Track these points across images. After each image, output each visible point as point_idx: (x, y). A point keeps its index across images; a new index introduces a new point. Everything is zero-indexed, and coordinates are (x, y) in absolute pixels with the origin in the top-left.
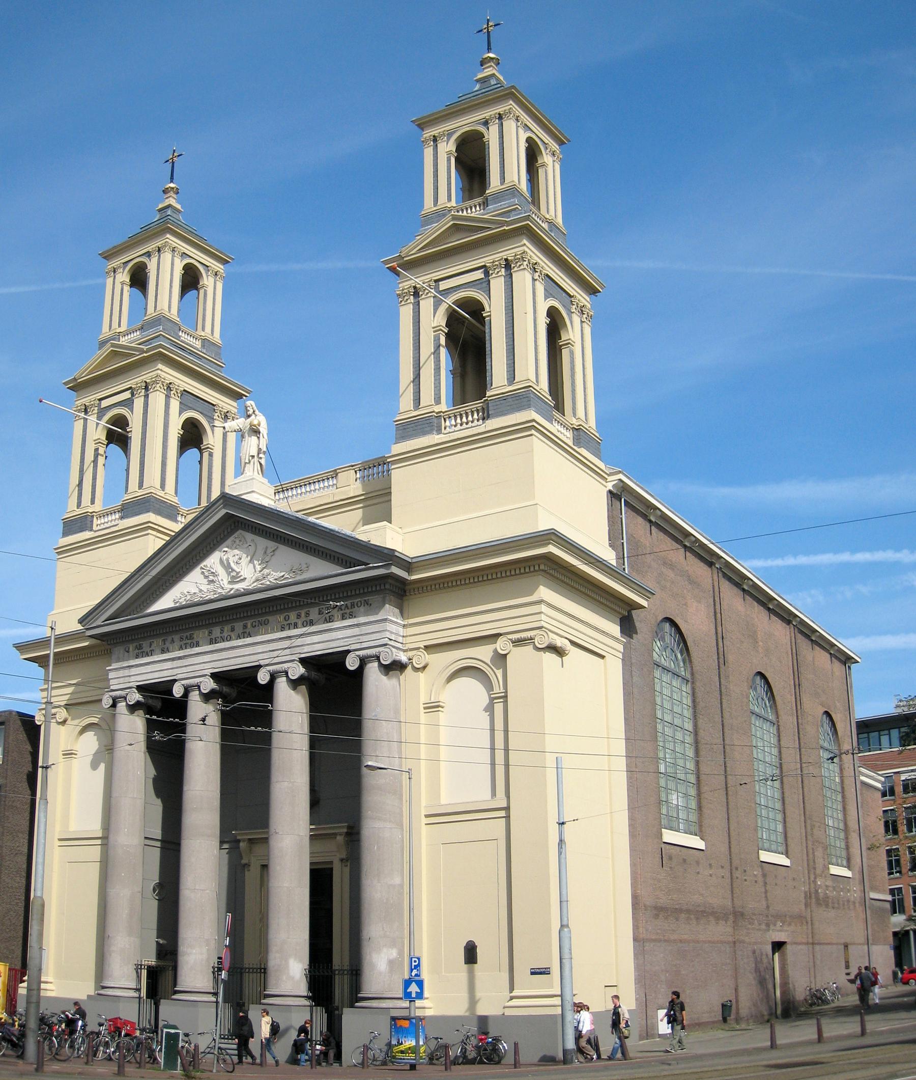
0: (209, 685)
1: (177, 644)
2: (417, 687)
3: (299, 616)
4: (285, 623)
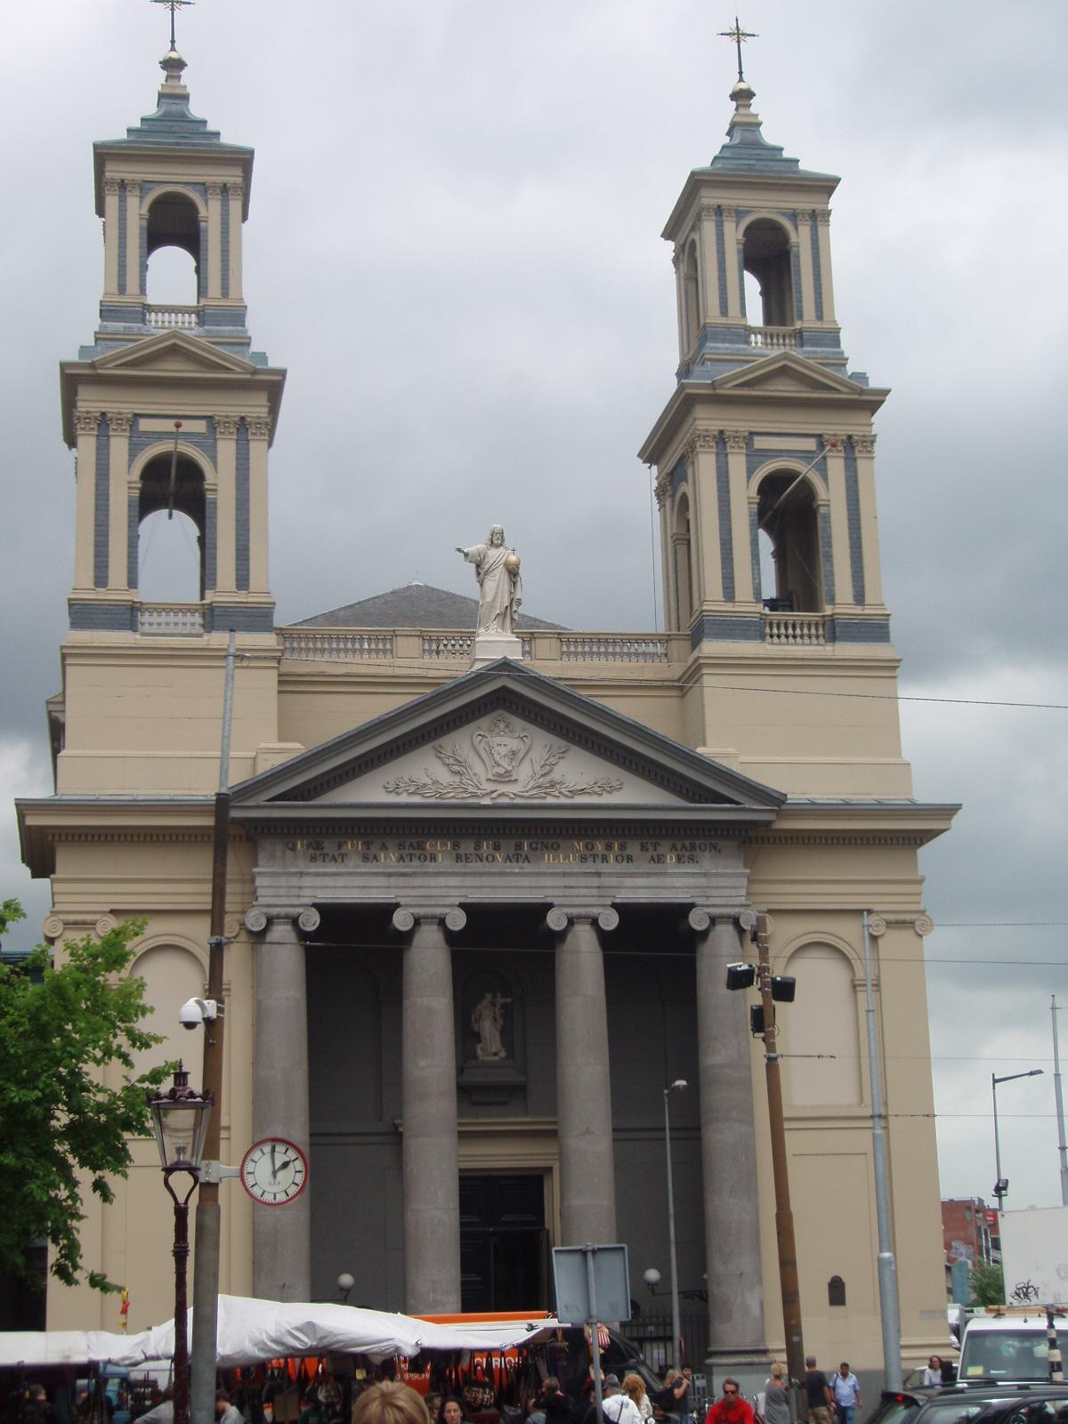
3: (609, 847)
4: (588, 853)
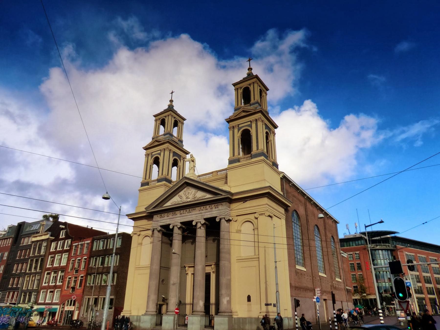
1: (171, 215)
2: (234, 226)
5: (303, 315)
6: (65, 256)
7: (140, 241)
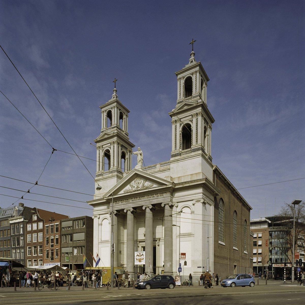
0: (132, 210)
5: (217, 274)
6: (40, 234)
7: (100, 223)
